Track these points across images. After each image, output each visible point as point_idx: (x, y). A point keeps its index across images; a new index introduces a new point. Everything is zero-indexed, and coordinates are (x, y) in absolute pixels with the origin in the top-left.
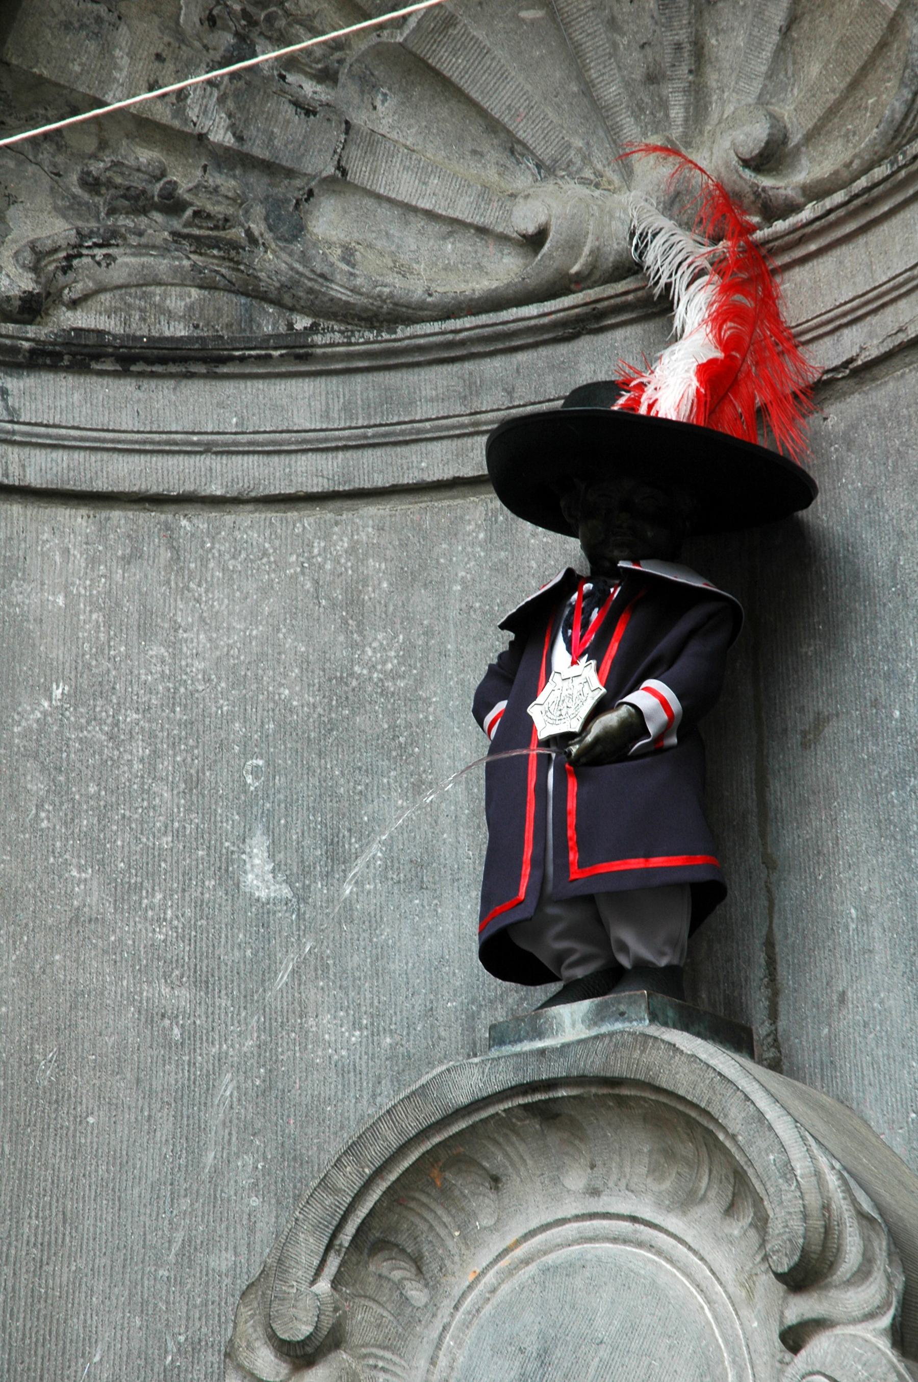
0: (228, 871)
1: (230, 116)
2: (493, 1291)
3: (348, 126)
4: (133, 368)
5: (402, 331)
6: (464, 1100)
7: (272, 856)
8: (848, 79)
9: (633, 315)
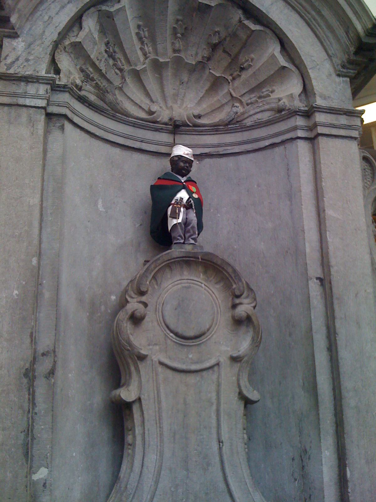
0: (96, 204)
1: (106, 68)
2: (171, 288)
3: (125, 80)
4: (90, 107)
5: (130, 119)
6: (175, 257)
7: (102, 203)
8: (212, 110)
9: (168, 132)
